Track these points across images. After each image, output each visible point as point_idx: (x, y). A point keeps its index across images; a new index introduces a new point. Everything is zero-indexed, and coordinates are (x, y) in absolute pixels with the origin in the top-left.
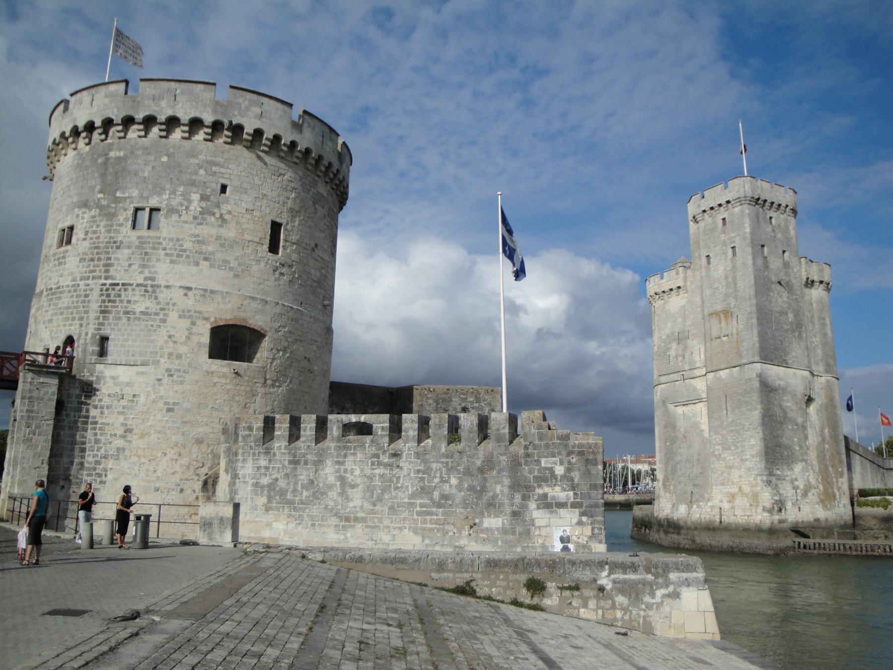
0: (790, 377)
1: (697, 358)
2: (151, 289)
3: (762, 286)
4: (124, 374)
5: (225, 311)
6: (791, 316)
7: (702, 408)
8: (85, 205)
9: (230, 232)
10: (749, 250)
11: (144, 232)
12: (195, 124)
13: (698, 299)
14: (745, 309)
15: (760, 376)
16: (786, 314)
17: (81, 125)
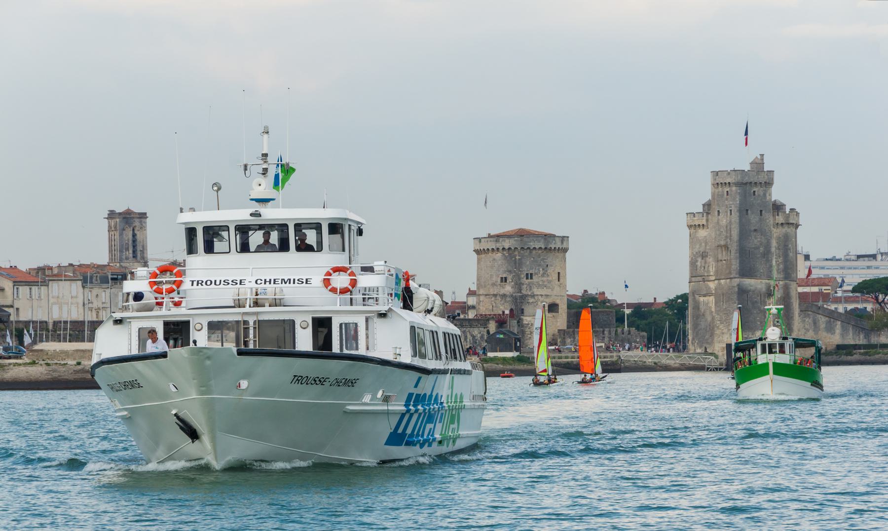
0: (755, 284)
1: (711, 269)
2: (533, 296)
3: (744, 233)
4: (529, 319)
5: (550, 301)
6: (762, 249)
7: (712, 299)
8: (510, 272)
9: (550, 279)
10: (738, 214)
11: (529, 280)
12: (540, 248)
13: (713, 235)
14: (734, 247)
15: (738, 285)
16: (758, 248)
17: (507, 247)
